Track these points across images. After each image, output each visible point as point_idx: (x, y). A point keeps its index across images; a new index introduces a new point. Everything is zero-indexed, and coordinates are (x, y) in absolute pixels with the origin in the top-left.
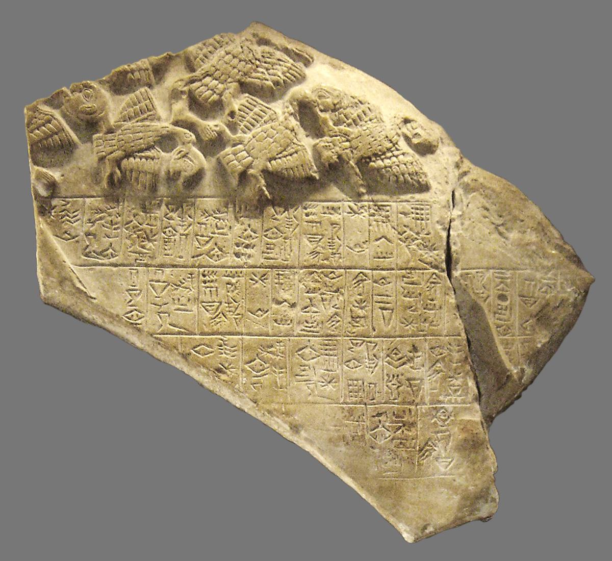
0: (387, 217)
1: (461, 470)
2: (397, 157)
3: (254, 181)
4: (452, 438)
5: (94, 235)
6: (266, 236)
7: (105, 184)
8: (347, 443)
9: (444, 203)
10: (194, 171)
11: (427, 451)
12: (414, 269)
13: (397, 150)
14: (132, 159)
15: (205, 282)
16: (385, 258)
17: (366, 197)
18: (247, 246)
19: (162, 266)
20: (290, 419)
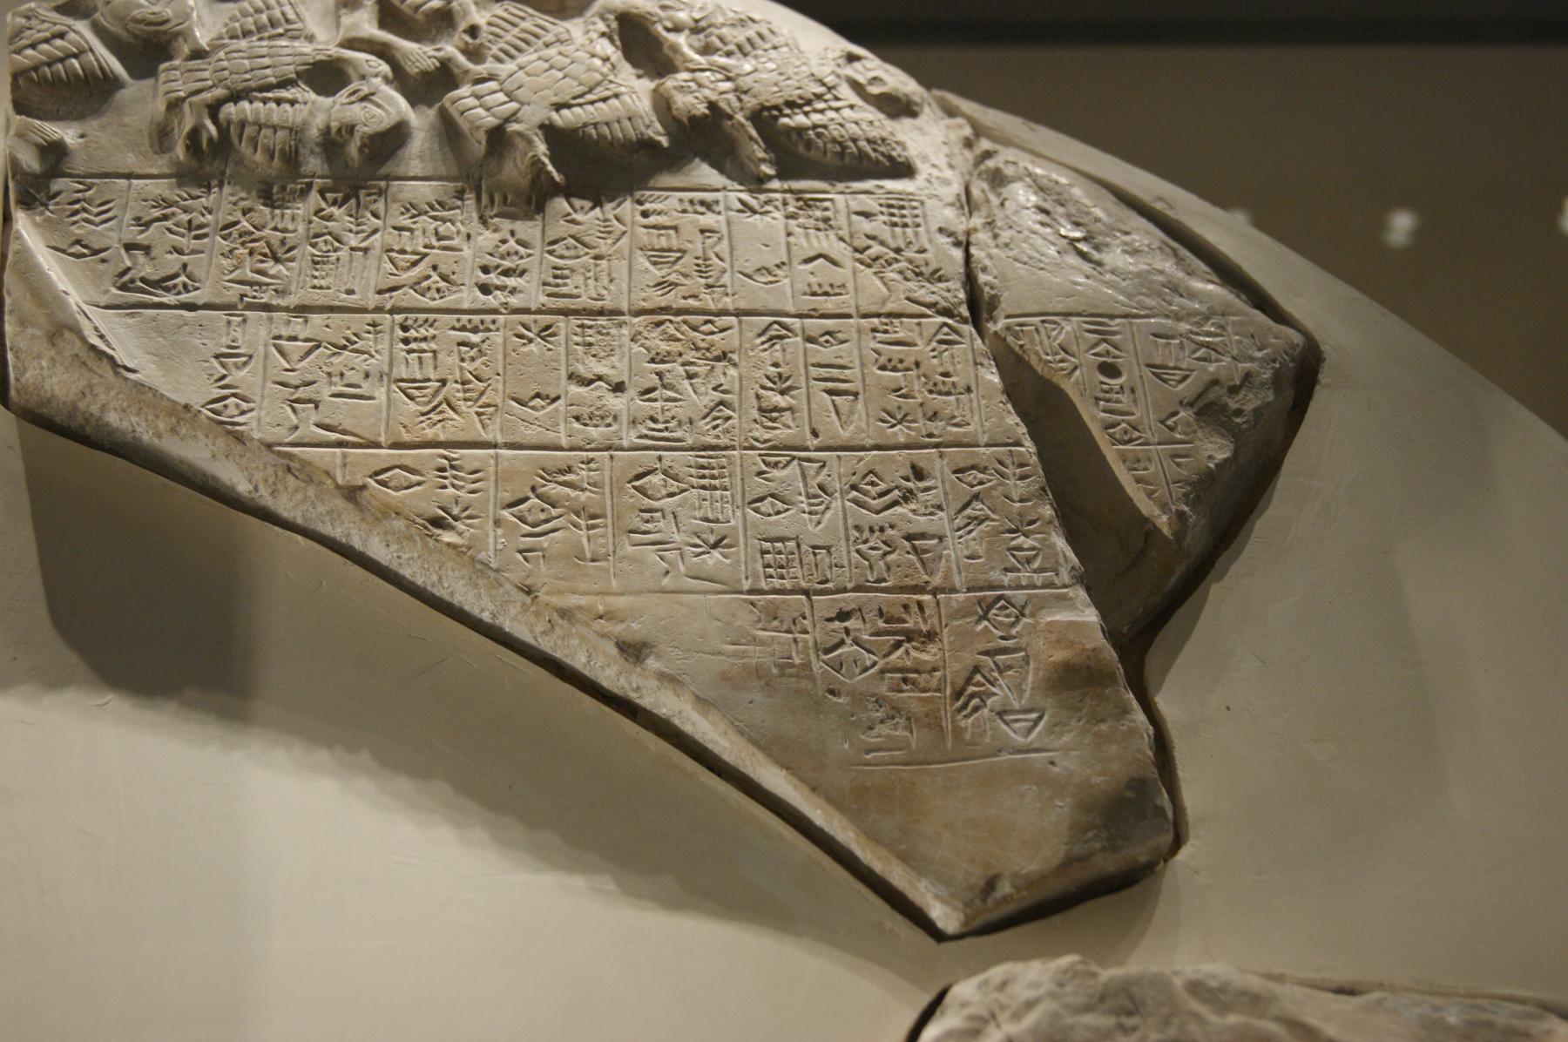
0: (826, 220)
1: (1067, 738)
2: (837, 110)
3: (521, 144)
4: (1032, 666)
5: (147, 249)
6: (551, 253)
7: (180, 152)
8: (767, 684)
9: (951, 199)
10: (386, 124)
11: (972, 696)
12: (899, 315)
13: (837, 99)
14: (245, 104)
15: (406, 341)
16: (826, 294)
17: (775, 184)
18: (507, 273)
19: (303, 310)
20: (619, 628)
